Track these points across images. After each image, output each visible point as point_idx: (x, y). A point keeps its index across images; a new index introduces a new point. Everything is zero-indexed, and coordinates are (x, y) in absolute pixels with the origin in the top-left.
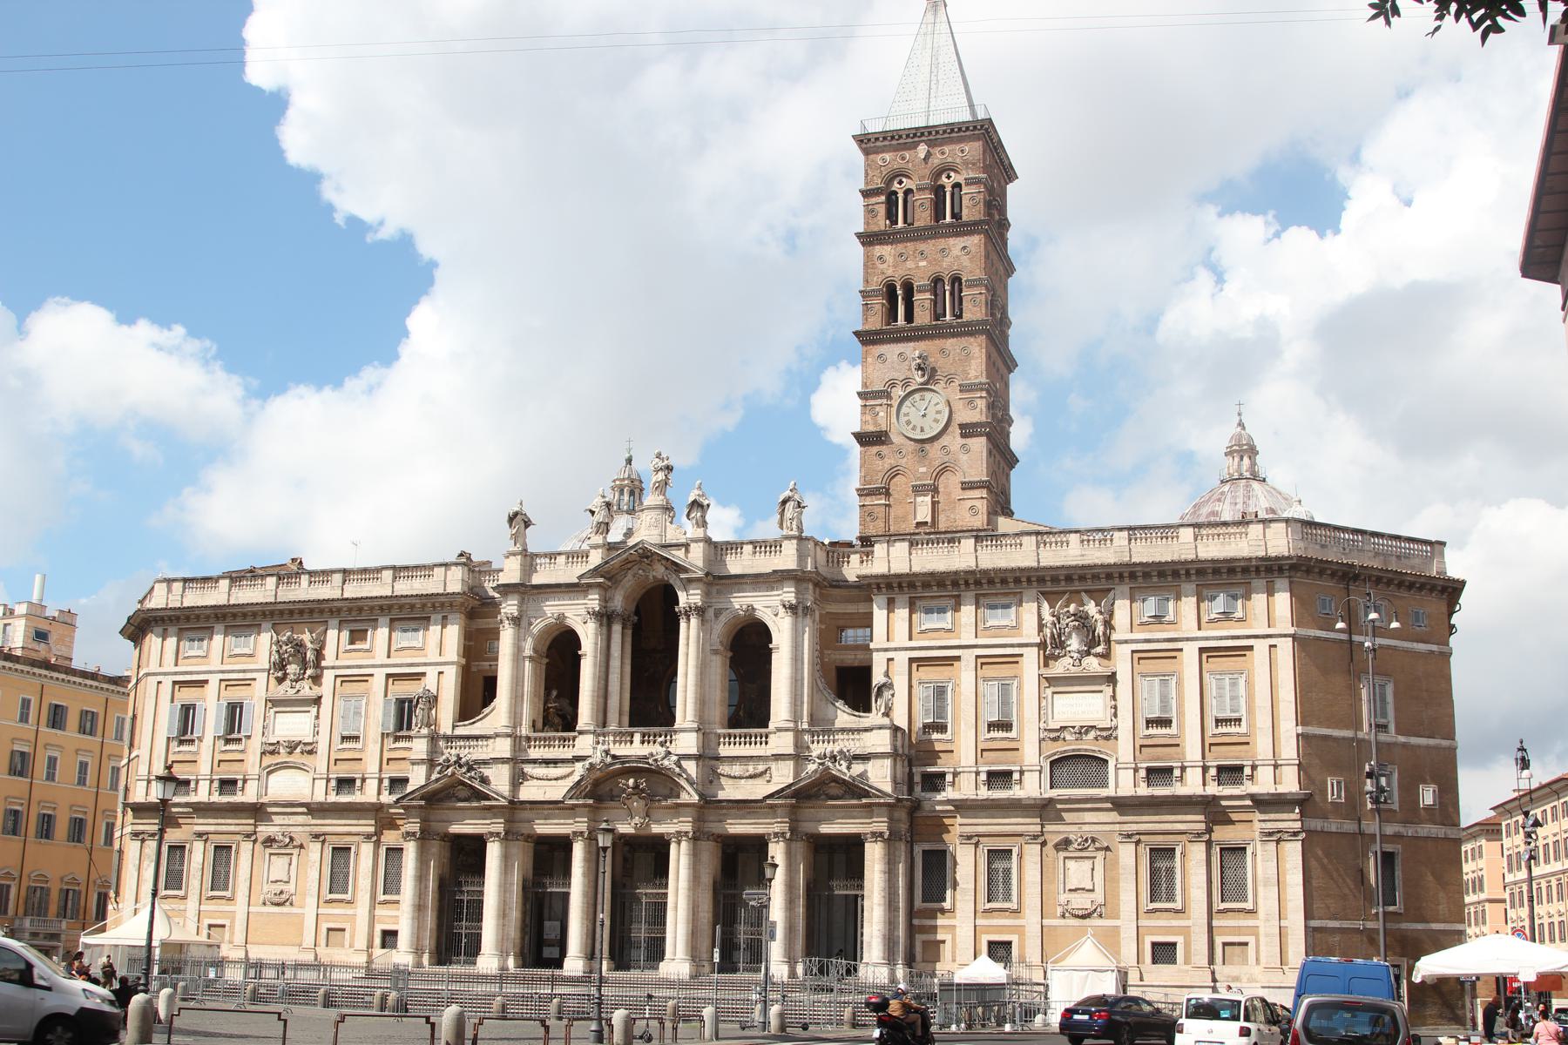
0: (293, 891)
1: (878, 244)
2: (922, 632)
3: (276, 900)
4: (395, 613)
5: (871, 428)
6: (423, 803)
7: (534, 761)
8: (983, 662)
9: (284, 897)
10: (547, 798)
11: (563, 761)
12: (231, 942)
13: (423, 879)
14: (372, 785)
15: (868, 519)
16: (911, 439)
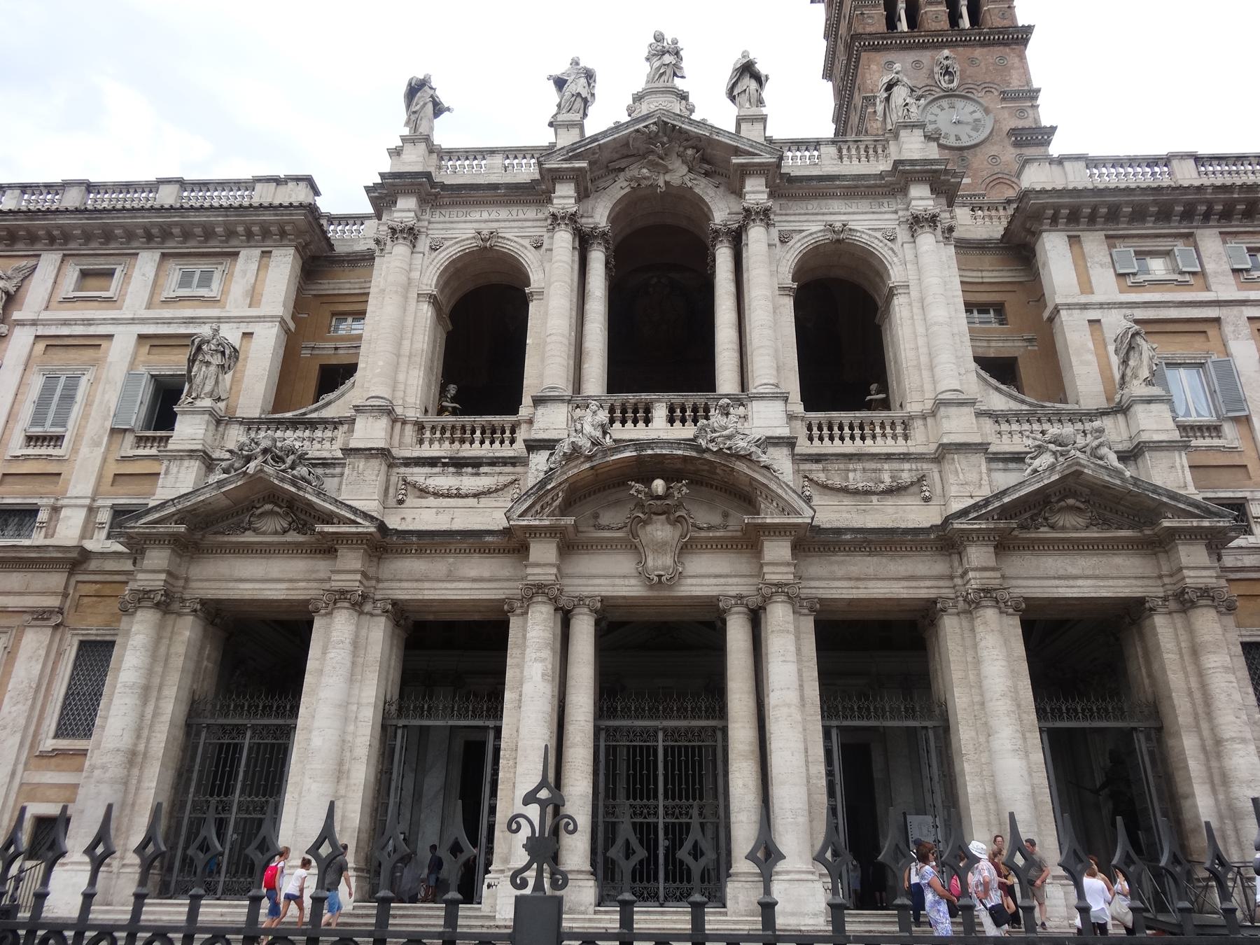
4: (172, 246)
6: (182, 528)
7: (432, 462)
10: (458, 525)
11: (493, 462)
13: (155, 694)
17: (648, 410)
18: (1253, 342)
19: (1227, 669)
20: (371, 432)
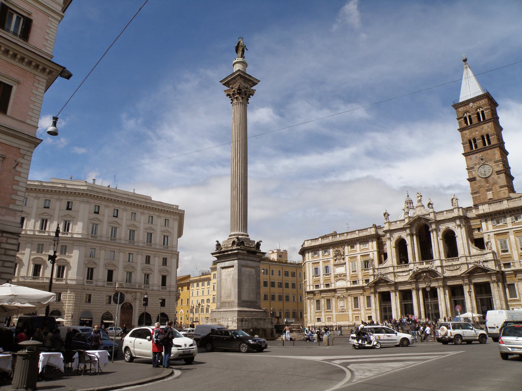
0: (346, 308)
2: (496, 227)
3: (342, 311)
5: (471, 177)
6: (374, 285)
8: (516, 232)
9: (344, 310)
11: (407, 271)
12: (333, 321)
14: (361, 282)
15: (475, 200)
17: (423, 263)
19: (496, 291)
20: (391, 270)
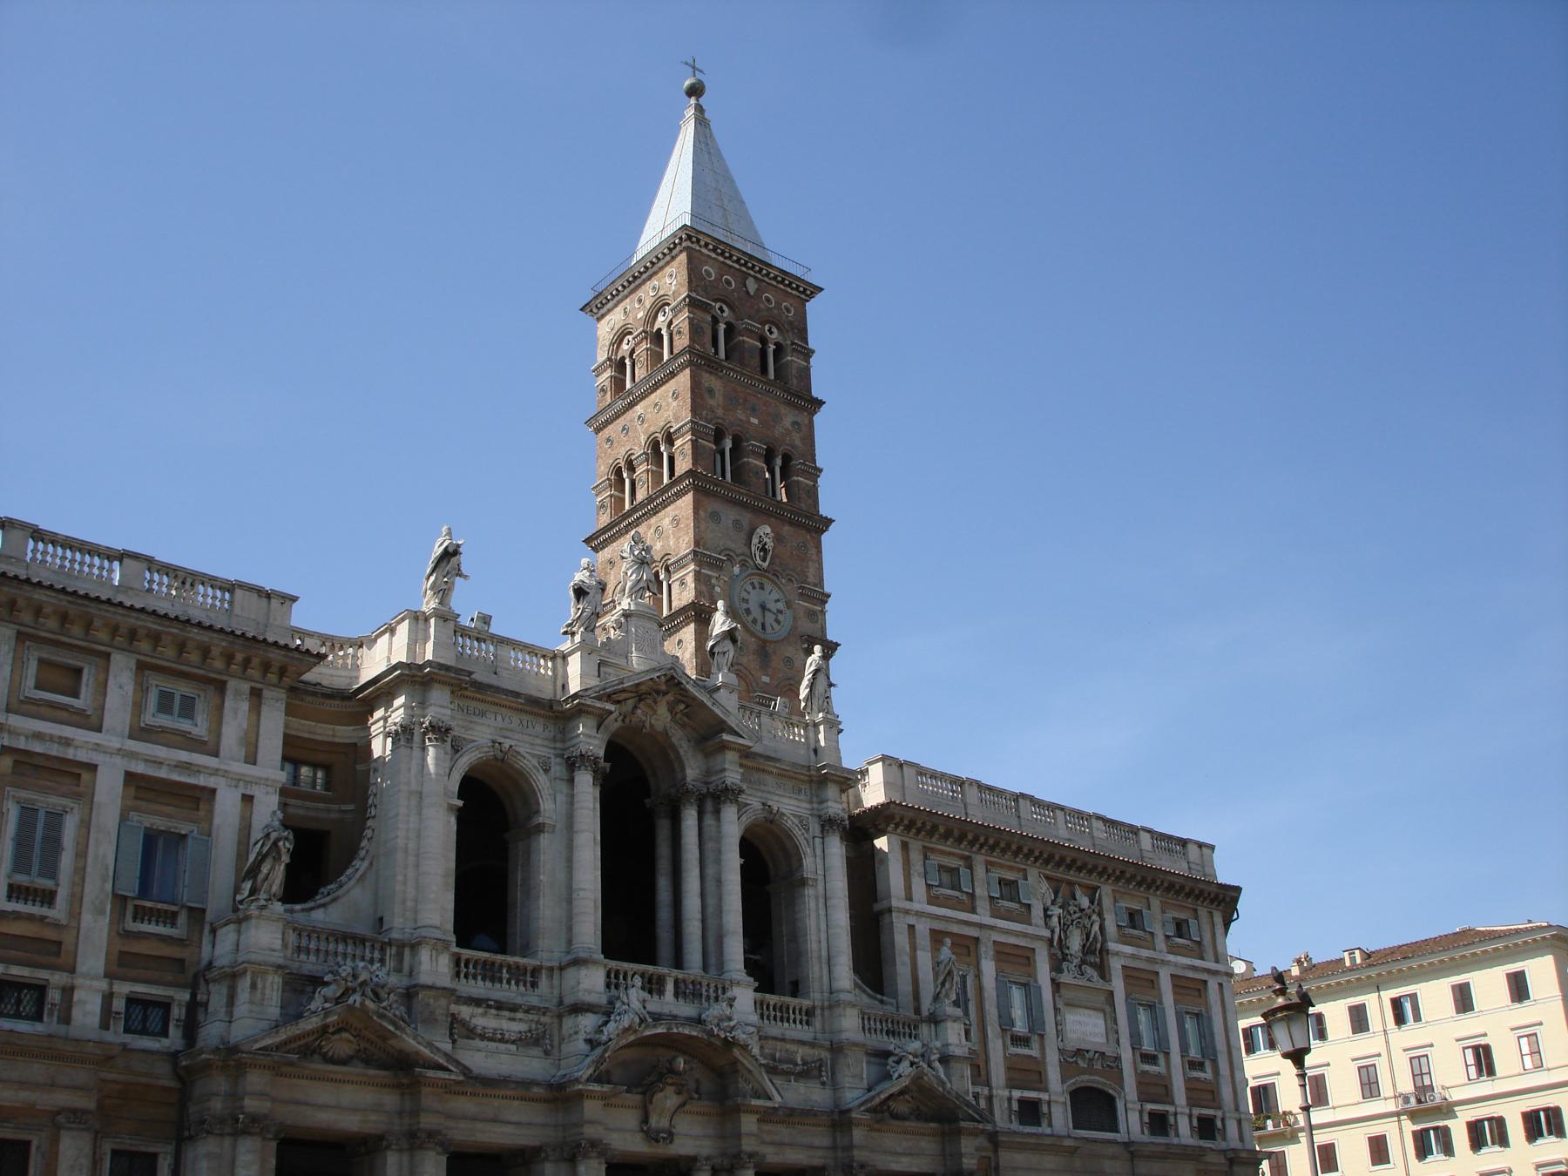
1: (706, 371)
16: (753, 634)
18: (994, 963)
